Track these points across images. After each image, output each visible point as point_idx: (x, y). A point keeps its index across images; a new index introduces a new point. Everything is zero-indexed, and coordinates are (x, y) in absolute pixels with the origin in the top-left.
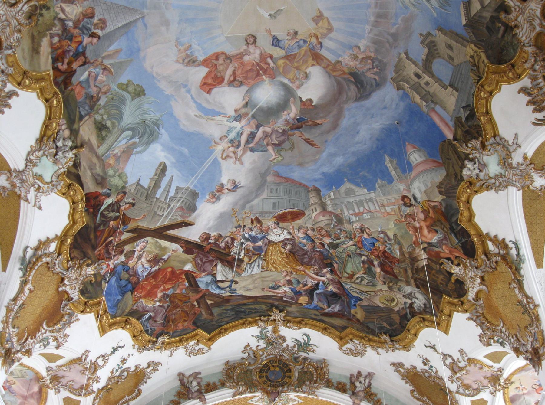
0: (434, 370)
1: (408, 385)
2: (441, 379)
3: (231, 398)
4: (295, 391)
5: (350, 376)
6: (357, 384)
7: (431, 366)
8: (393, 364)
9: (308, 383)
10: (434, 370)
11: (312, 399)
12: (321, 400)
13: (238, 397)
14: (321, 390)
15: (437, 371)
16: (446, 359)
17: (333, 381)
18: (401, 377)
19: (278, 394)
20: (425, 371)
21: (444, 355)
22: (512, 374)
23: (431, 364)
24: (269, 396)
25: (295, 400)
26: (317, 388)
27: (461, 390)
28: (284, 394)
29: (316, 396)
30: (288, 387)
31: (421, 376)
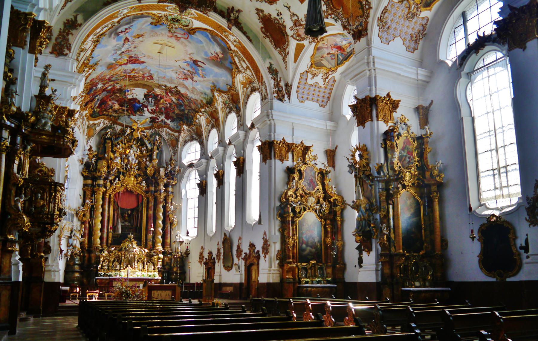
0: (282, 20)
1: (261, 24)
2: (285, 27)
3: (156, 4)
4: (196, 9)
5: (227, 8)
6: (232, 15)
7: (282, 18)
8: (257, 9)
9: (204, 6)
10: (282, 20)
11: (204, 17)
12: (210, 19)
13: (161, 4)
14: (211, 13)
15: (284, 22)
16: (294, 17)
17: (218, 9)
18: (259, 18)
19: (186, 9)
20: (275, 19)
21: (294, 14)
22: (327, 36)
23: (282, 16)
24: (180, 9)
25: (194, 15)
26: (209, 11)
27: (295, 36)
28: (189, 9)
29: (208, 16)
30: (192, 5)
31: (272, 21)
